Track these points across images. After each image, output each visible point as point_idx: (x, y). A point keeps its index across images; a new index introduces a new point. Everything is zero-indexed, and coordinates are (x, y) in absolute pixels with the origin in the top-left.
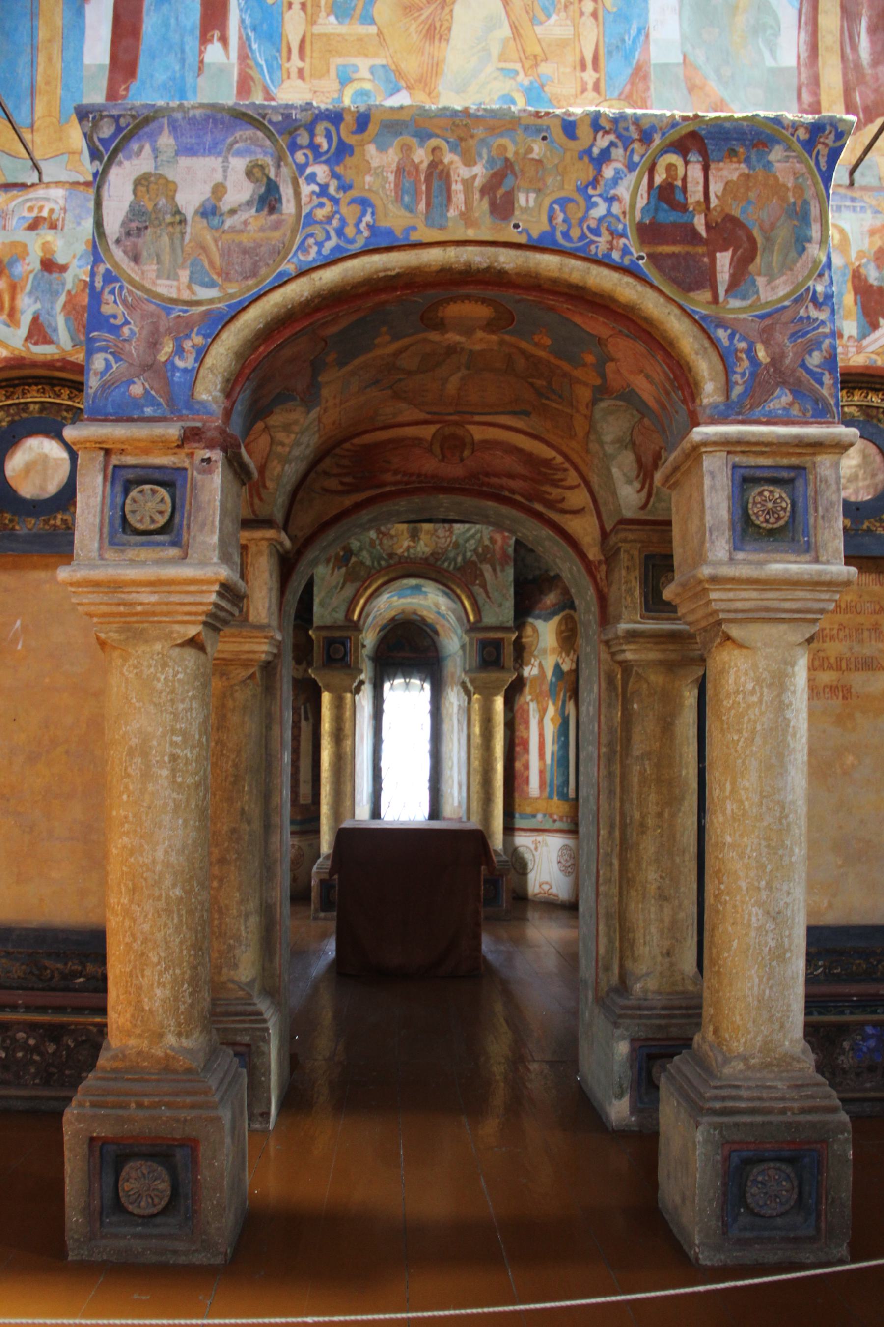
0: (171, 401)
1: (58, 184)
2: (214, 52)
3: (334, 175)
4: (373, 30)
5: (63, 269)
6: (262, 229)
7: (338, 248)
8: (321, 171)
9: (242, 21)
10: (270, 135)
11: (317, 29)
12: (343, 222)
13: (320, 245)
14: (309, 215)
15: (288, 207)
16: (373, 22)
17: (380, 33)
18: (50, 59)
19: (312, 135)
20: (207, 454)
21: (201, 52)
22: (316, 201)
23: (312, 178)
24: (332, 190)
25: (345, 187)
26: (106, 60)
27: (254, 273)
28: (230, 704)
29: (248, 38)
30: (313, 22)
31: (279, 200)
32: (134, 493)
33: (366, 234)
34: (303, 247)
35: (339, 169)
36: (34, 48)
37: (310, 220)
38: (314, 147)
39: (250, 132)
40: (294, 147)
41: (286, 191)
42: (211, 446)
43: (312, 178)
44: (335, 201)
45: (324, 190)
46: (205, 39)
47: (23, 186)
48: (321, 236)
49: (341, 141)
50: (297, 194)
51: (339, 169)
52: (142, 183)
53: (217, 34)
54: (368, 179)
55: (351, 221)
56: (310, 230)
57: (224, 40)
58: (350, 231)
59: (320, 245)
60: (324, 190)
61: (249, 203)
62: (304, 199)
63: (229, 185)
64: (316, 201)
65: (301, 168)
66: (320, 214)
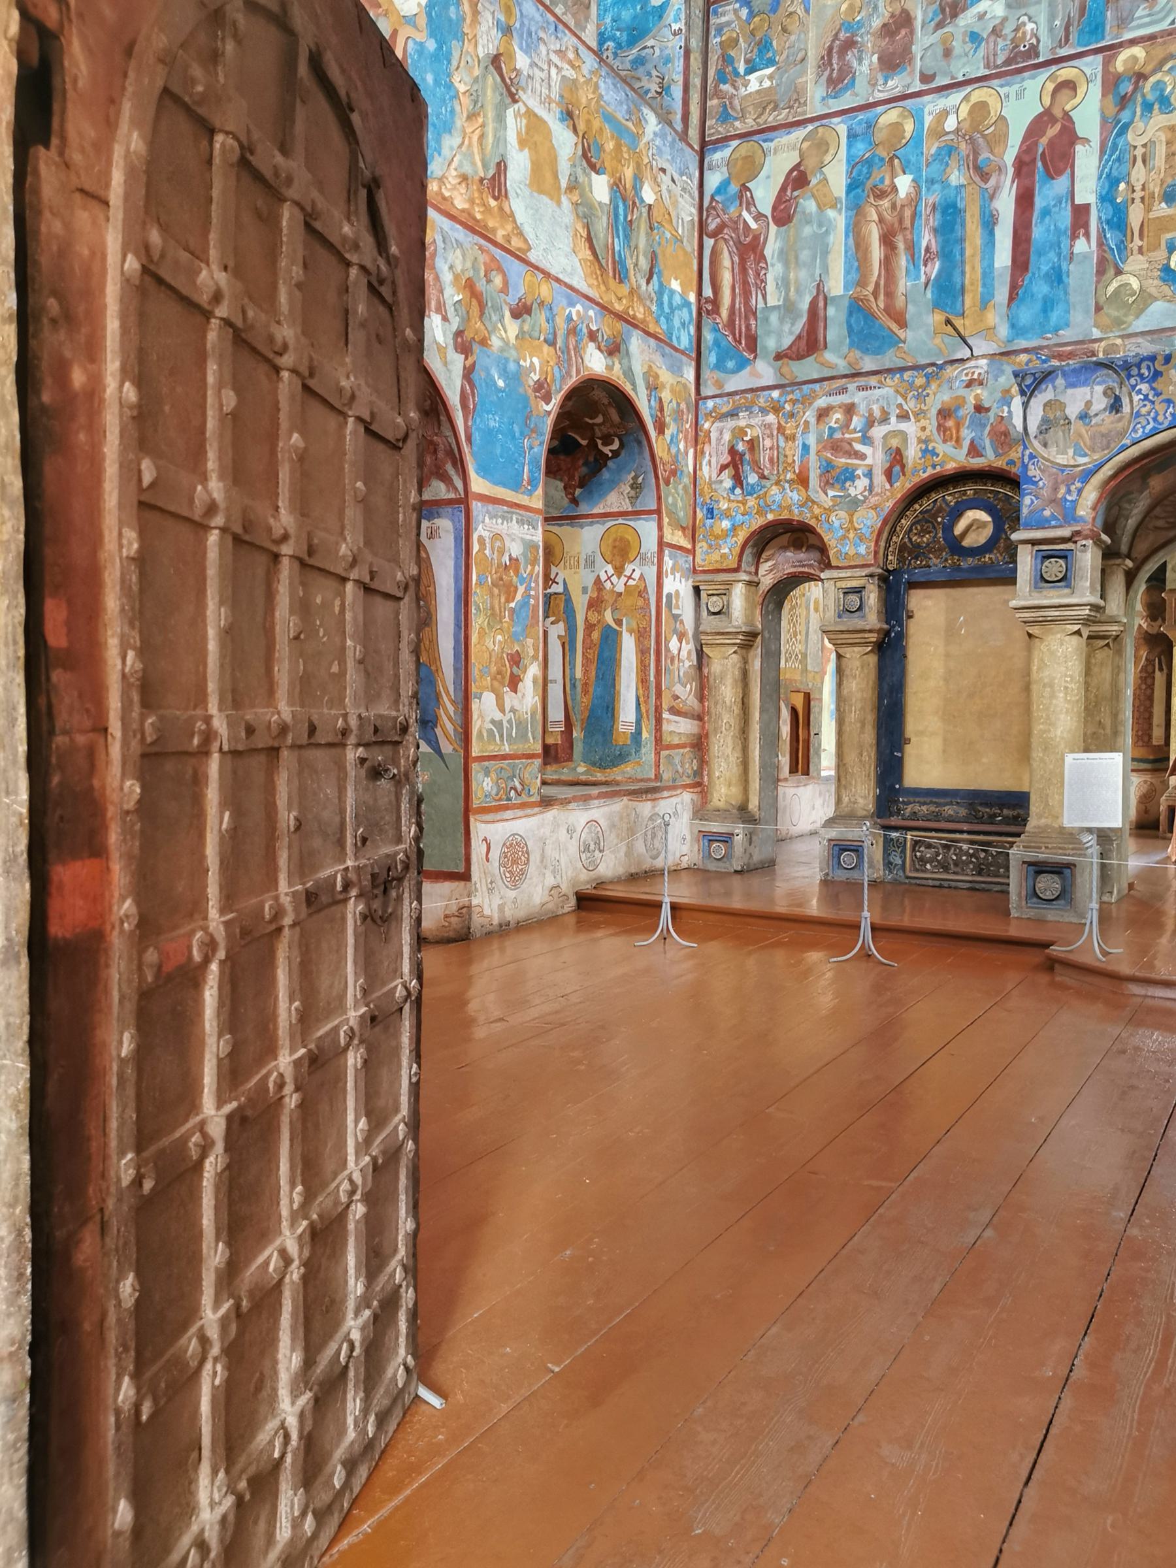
0: (1065, 517)
1: (983, 356)
2: (1081, 246)
3: (1152, 389)
5: (988, 410)
6: (1112, 423)
7: (1154, 428)
8: (1144, 387)
9: (1100, 218)
10: (1116, 372)
11: (1152, 215)
12: (1157, 414)
13: (1144, 427)
14: (1138, 411)
15: (1126, 409)
18: (973, 268)
19: (1139, 369)
20: (1084, 542)
21: (1072, 246)
22: (1142, 403)
23: (1139, 392)
24: (1150, 397)
25: (1158, 394)
26: (1010, 264)
27: (1108, 448)
28: (1093, 661)
29: (1104, 230)
31: (1121, 406)
32: (1046, 563)
33: (1170, 418)
34: (1135, 430)
35: (1154, 385)
36: (963, 262)
37: (1138, 414)
38: (1141, 375)
39: (1105, 371)
40: (1129, 376)
41: (1125, 401)
42: (1086, 538)
43: (1139, 392)
44: (1153, 403)
45: (1146, 397)
46: (1074, 237)
47: (962, 360)
48: (1144, 423)
49: (1155, 370)
50: (1131, 401)
51: (1154, 385)
52: (1047, 405)
53: (1082, 231)
54: (1171, 388)
55: (1161, 413)
56: (1138, 420)
57: (1087, 235)
58: (1161, 418)
59: (1144, 427)
60: (1146, 397)
61: (1105, 410)
62: (1135, 403)
63: (1094, 401)
64: (1142, 403)
65: (1134, 387)
66: (1144, 411)
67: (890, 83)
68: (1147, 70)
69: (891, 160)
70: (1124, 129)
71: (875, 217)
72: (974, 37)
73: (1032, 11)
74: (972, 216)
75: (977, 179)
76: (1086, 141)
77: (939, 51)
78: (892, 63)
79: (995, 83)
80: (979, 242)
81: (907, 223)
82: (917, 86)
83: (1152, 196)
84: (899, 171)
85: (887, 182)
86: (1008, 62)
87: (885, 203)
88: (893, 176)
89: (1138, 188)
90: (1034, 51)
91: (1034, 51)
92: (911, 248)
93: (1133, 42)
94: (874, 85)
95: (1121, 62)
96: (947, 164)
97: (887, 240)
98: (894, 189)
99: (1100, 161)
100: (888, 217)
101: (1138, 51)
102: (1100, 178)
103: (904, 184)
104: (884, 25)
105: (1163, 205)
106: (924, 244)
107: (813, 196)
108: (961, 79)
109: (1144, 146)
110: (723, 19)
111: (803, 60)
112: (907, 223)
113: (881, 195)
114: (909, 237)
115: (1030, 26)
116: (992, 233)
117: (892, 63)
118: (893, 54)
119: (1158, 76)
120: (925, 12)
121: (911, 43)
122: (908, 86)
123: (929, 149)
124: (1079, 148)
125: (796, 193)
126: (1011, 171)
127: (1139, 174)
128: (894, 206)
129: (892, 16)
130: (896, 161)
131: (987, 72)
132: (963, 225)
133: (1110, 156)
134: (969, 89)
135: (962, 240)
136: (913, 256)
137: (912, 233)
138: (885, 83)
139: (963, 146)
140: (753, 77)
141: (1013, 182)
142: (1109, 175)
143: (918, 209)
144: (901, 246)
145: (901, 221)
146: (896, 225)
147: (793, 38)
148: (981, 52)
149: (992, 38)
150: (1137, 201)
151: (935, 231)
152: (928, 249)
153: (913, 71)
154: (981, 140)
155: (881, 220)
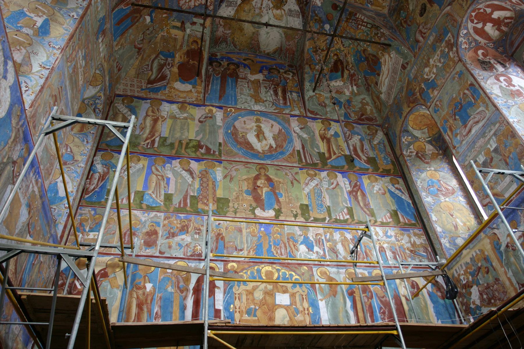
4: (256, 318)
9: (224, 316)
11: (243, 318)
16: (256, 316)
17: (258, 319)
30: (242, 316)
67: (147, 251)
68: (238, 271)
69: (145, 277)
70: (231, 288)
71: (135, 296)
72: (180, 245)
73: (200, 243)
74: (176, 304)
75: (179, 291)
76: (219, 288)
77: (167, 245)
78: (149, 244)
79: (186, 261)
80: (178, 315)
81: (149, 301)
82: (158, 254)
83: (242, 311)
84: (148, 281)
85: (142, 284)
86: (191, 256)
87: (140, 292)
88: (145, 282)
89: (237, 308)
90: (200, 255)
91: (200, 255)
92: (150, 312)
93: (233, 261)
94: (141, 249)
95: (230, 265)
96: (167, 284)
97: (140, 306)
98: (145, 288)
99: (224, 295)
100: (141, 297)
101: (234, 264)
102: (224, 301)
103: (149, 286)
104: (147, 232)
105: (246, 315)
106: (155, 311)
107: (109, 282)
108: (174, 256)
109: (239, 294)
110: (83, 212)
111: (114, 234)
112: (149, 301)
113: (139, 288)
114: (149, 307)
115: (199, 247)
116: (183, 312)
117: (149, 244)
118: (149, 242)
119: (242, 273)
120: (163, 233)
121: (157, 240)
122: (154, 253)
123: (160, 276)
124: (216, 290)
125: (101, 279)
126: (192, 292)
127: (237, 302)
128: (144, 294)
129: (150, 230)
130: (147, 278)
131: (184, 257)
132: (172, 307)
133: (227, 295)
134: (177, 260)
135: (171, 313)
136: (150, 315)
137: (151, 306)
138: (146, 250)
139: (174, 279)
140: (91, 233)
141: (192, 295)
142: (227, 301)
143: (154, 297)
144: (145, 310)
145: (146, 300)
146: (144, 301)
147: (111, 226)
148: (182, 250)
149: (186, 247)
150: (238, 312)
151: (160, 307)
152: (157, 313)
153: (156, 249)
154: (180, 278)
155: (138, 298)
